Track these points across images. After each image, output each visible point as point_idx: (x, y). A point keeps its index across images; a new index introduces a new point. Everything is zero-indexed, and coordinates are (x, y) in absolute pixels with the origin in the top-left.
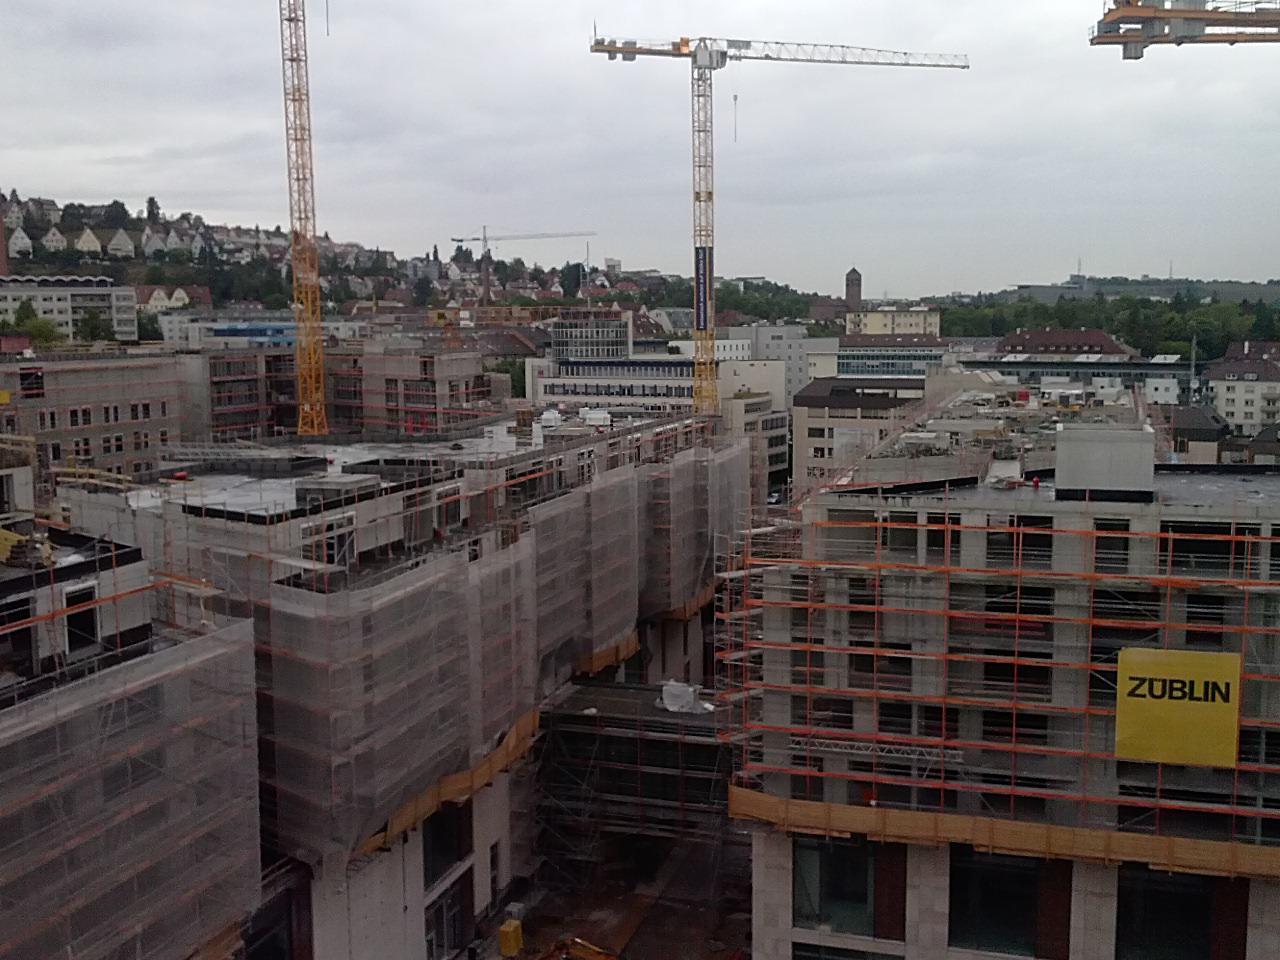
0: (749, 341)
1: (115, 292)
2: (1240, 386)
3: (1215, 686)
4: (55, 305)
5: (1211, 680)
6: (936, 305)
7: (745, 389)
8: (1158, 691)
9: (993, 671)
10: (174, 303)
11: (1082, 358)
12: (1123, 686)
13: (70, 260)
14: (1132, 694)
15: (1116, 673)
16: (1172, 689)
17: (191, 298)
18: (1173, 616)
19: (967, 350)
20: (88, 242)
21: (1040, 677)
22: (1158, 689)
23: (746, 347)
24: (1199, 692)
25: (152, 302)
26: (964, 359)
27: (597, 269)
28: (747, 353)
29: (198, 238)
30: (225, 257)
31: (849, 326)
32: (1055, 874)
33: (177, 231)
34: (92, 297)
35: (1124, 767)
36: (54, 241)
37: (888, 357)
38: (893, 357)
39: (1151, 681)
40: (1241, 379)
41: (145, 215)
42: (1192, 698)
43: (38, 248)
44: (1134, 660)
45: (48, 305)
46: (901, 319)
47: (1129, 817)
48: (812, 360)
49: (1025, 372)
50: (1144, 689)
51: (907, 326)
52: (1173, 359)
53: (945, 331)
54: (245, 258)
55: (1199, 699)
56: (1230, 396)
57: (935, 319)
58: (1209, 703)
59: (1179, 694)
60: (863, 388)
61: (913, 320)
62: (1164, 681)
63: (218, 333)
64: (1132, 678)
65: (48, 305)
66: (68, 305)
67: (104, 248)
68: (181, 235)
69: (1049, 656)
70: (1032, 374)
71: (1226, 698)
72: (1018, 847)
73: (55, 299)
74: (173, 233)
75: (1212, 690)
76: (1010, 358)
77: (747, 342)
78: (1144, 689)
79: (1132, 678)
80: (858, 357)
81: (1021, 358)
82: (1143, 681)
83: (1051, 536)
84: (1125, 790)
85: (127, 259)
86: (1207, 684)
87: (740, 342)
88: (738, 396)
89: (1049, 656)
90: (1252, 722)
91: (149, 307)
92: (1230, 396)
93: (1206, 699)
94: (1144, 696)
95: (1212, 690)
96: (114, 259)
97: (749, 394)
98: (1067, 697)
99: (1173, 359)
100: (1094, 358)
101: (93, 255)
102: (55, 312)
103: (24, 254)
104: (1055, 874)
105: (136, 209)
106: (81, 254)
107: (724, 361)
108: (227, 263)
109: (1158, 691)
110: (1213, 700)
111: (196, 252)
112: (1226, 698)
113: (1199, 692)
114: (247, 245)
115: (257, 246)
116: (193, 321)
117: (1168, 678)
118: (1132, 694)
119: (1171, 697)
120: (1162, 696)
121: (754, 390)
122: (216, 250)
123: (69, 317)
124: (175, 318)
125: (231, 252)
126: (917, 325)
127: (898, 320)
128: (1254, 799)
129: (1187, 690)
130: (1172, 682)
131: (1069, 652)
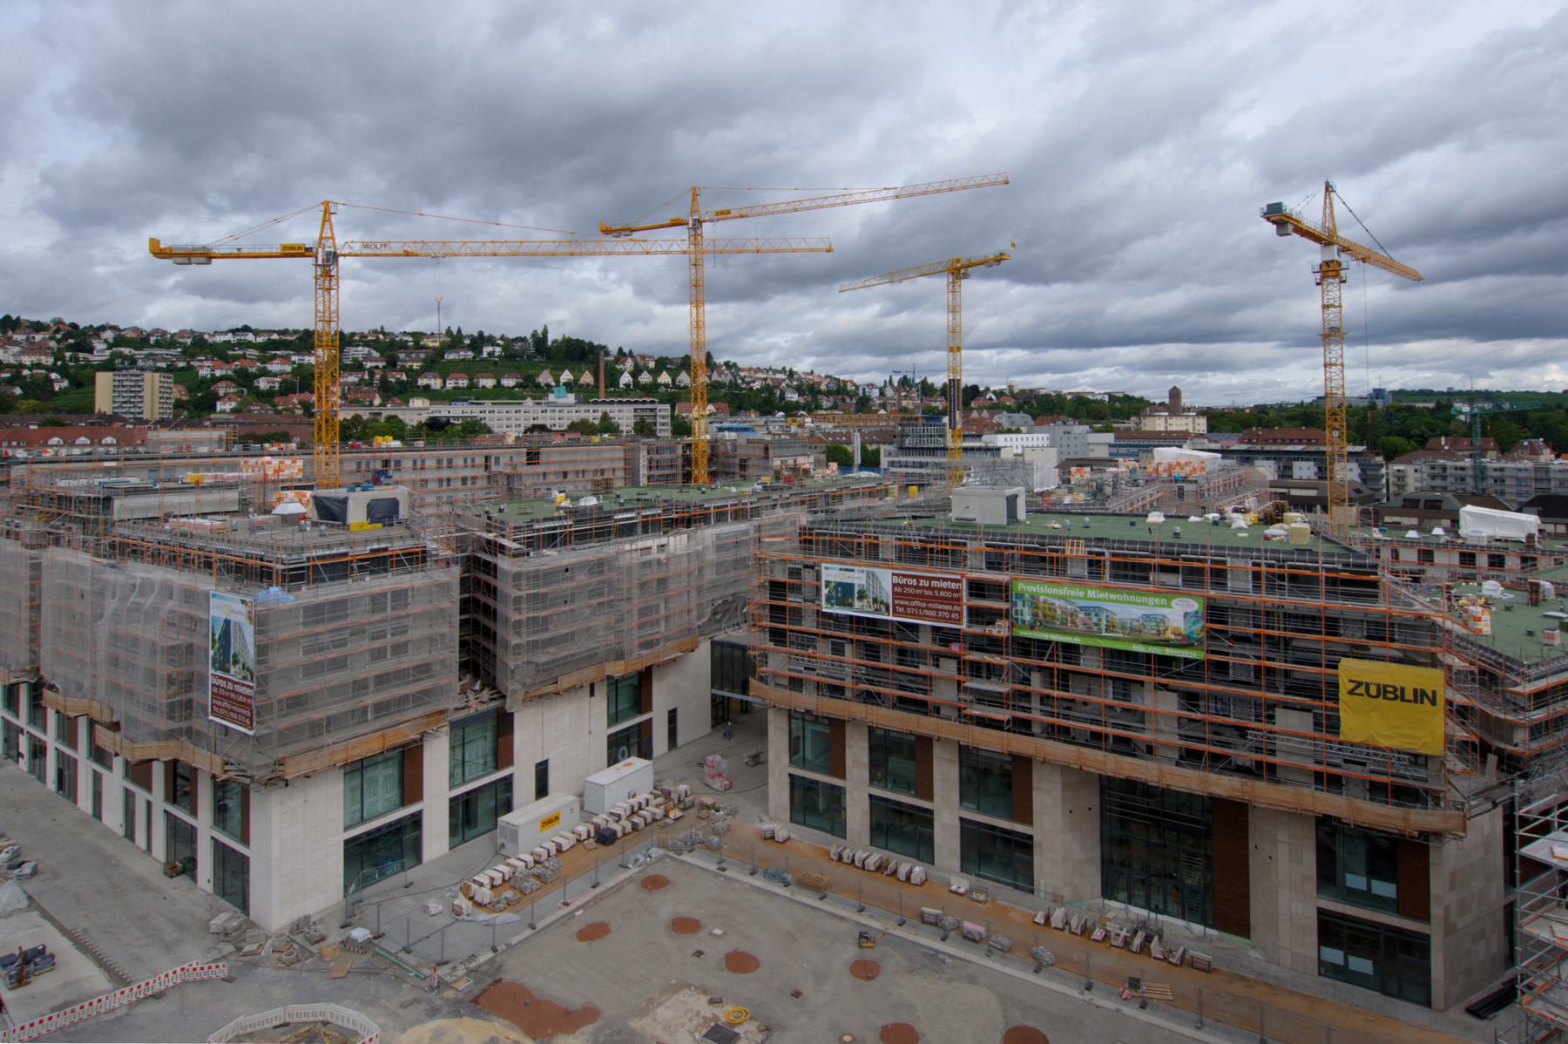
13: (651, 389)
20: (665, 378)
22: (1373, 691)
36: (645, 378)
43: (636, 383)
59: (1392, 696)
67: (674, 381)
85: (685, 387)
96: (678, 387)
101: (666, 386)
103: (627, 385)
117: (1382, 682)
120: (1377, 696)
127: (1169, 422)
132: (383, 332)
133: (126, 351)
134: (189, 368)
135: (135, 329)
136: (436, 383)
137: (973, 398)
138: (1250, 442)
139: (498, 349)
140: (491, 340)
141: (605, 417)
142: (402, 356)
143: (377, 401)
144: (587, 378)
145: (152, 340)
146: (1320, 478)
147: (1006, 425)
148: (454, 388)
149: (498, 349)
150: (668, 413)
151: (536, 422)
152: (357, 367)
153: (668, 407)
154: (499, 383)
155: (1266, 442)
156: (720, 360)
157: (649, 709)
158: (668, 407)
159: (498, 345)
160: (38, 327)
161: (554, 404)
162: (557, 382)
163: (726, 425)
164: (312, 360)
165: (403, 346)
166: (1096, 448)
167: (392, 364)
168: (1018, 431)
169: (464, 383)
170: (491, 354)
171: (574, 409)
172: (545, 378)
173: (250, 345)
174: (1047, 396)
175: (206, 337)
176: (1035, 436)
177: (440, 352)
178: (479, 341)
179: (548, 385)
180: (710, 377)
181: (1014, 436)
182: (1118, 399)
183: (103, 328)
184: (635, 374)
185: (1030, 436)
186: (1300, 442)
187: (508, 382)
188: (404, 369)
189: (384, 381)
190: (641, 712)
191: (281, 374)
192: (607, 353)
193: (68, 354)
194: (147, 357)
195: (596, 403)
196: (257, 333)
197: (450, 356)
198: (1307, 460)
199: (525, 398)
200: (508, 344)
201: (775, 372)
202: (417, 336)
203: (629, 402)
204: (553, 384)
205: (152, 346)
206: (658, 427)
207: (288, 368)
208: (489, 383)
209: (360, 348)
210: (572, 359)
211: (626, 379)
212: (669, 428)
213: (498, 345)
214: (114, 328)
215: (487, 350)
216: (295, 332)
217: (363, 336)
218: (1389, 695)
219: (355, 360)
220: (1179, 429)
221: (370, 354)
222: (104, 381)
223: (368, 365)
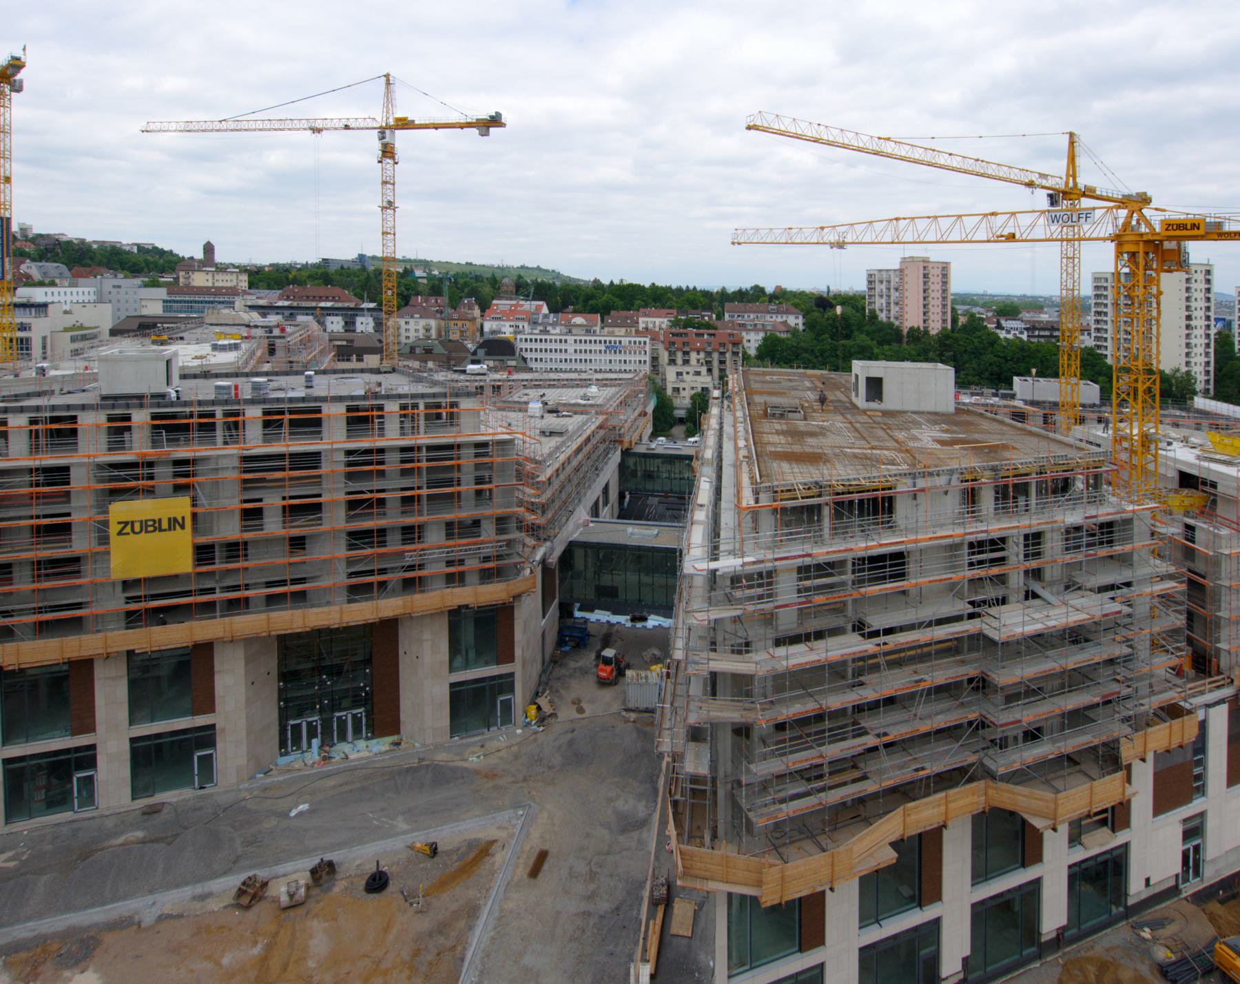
0: (95, 289)
2: (412, 321)
3: (175, 520)
5: (172, 516)
6: (243, 269)
7: (79, 324)
8: (137, 528)
9: (38, 531)
11: (323, 304)
12: (114, 529)
14: (120, 533)
15: (108, 521)
16: (147, 526)
18: (164, 476)
19: (252, 300)
21: (64, 530)
22: (137, 527)
23: (92, 293)
24: (165, 525)
26: (249, 304)
28: (93, 298)
31: (181, 280)
32: (83, 668)
35: (127, 584)
37: (188, 302)
38: (191, 302)
39: (133, 523)
40: (412, 317)
42: (161, 530)
44: (120, 510)
46: (220, 277)
47: (132, 619)
48: (144, 303)
49: (287, 313)
50: (128, 529)
51: (224, 281)
52: (372, 305)
53: (251, 285)
55: (165, 530)
56: (407, 327)
57: (245, 277)
58: (172, 532)
60: (162, 323)
61: (229, 277)
62: (141, 522)
64: (119, 523)
69: (69, 515)
70: (291, 314)
71: (183, 527)
72: (39, 659)
75: (174, 523)
76: (280, 304)
77: (92, 290)
78: (128, 529)
79: (119, 523)
80: (177, 302)
81: (286, 303)
82: (126, 523)
83: (6, 432)
84: (129, 600)
86: (169, 519)
87: (86, 290)
88: (66, 330)
89: (69, 515)
90: (202, 540)
92: (407, 327)
93: (170, 529)
94: (128, 534)
95: (174, 523)
97: (81, 327)
98: (80, 544)
99: (372, 305)
100: (329, 304)
104: (83, 668)
107: (53, 303)
109: (137, 528)
110: (175, 529)
112: (183, 527)
113: (165, 525)
117: (144, 518)
118: (120, 533)
119: (147, 532)
120: (141, 531)
121: (86, 325)
126: (231, 281)
128: (214, 589)
129: (157, 525)
130: (146, 521)
131: (81, 512)
138: (288, 299)
146: (346, 331)
155: (301, 299)
166: (149, 304)
168: (53, 284)
174: (69, 243)
176: (80, 290)
181: (49, 290)
182: (148, 251)
185: (69, 290)
186: (327, 299)
198: (337, 315)
218: (151, 529)
220: (229, 284)
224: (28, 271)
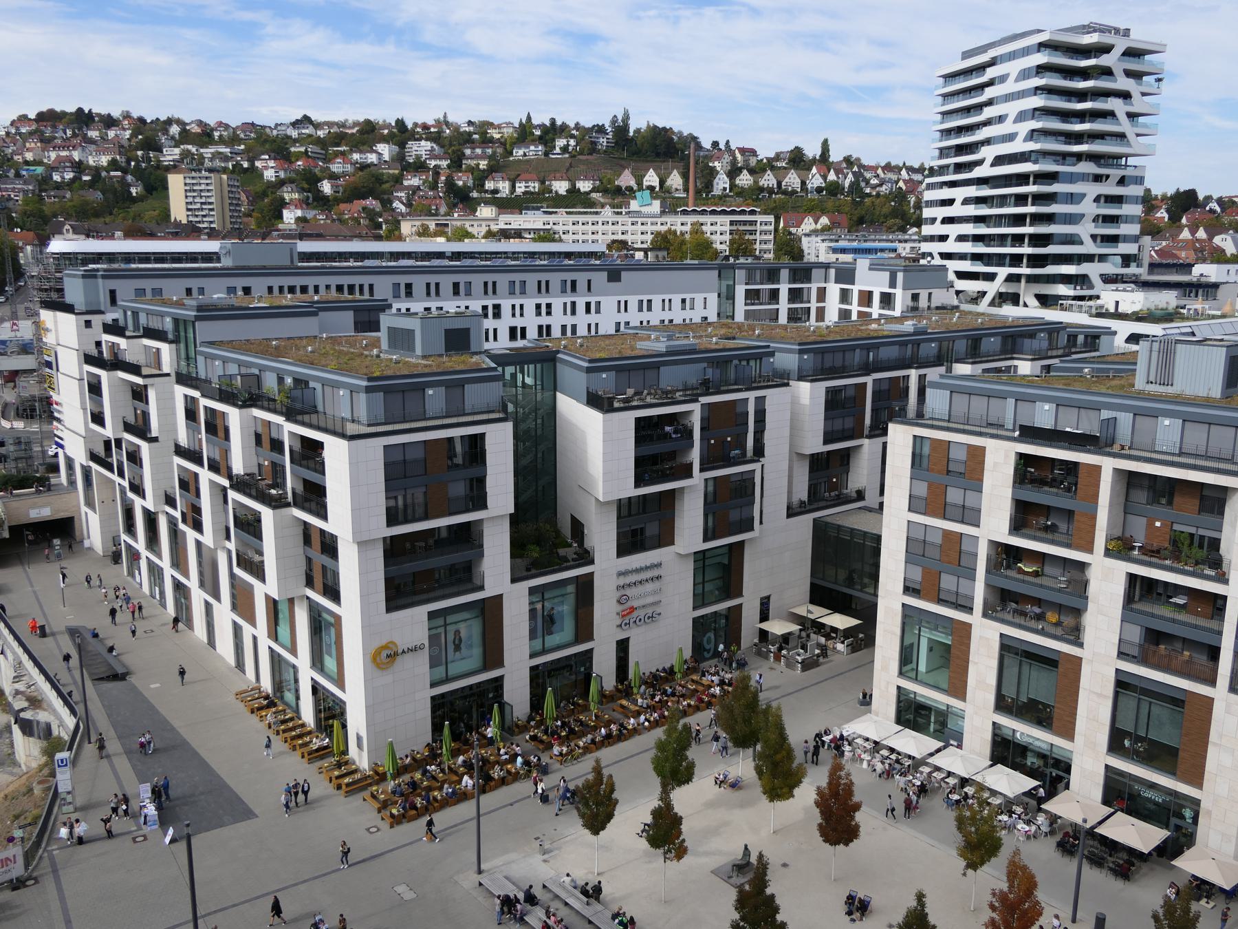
1: (759, 218)
4: (718, 228)
10: (819, 227)
17: (833, 223)
20: (769, 180)
25: (803, 226)
27: (1192, 194)
29: (850, 176)
30: (868, 190)
33: (835, 170)
34: (745, 223)
36: (745, 179)
41: (818, 158)
45: (714, 228)
54: (884, 189)
63: (835, 251)
65: (714, 228)
66: (727, 228)
67: (779, 184)
68: (837, 173)
73: (600, 223)
74: (832, 171)
91: (800, 230)
96: (785, 193)
101: (770, 191)
102: (600, 233)
105: (812, 150)
106: (762, 189)
108: (869, 195)
111: (847, 184)
114: (890, 181)
115: (897, 182)
116: (823, 240)
122: (863, 184)
123: (727, 237)
124: (813, 238)
125: (874, 187)
132: (447, 123)
133: (193, 149)
134: (253, 168)
135: (200, 123)
136: (504, 187)
137: (1185, 210)
139: (572, 142)
140: (563, 130)
141: (697, 229)
142: (468, 152)
143: (443, 210)
144: (675, 180)
145: (216, 134)
147: (1230, 249)
148: (525, 193)
149: (572, 142)
150: (772, 228)
151: (615, 237)
152: (419, 166)
153: (771, 218)
154: (574, 185)
156: (835, 156)
157: (739, 594)
158: (771, 218)
159: (572, 136)
160: (109, 122)
161: (638, 214)
162: (640, 183)
163: (843, 244)
164: (372, 158)
165: (466, 139)
167: (457, 163)
169: (535, 186)
170: (565, 149)
171: (659, 220)
172: (626, 179)
173: (310, 139)
175: (268, 130)
177: (507, 146)
178: (553, 131)
179: (630, 189)
180: (825, 177)
183: (169, 122)
184: (733, 172)
187: (584, 186)
188: (471, 170)
189: (450, 184)
190: (729, 596)
191: (344, 174)
192: (699, 146)
193: (140, 153)
194: (216, 155)
195: (685, 212)
196: (317, 126)
197: (519, 153)
199: (603, 206)
200: (588, 136)
201: (911, 170)
202: (484, 126)
203: (724, 212)
204: (635, 187)
205: (216, 143)
206: (757, 246)
207: (349, 168)
208: (561, 187)
209: (423, 143)
210: (658, 155)
211: (721, 183)
212: (771, 246)
213: (572, 136)
214: (179, 122)
215: (561, 143)
216: (356, 124)
217: (425, 127)
219: (418, 157)
221: (432, 150)
222: (176, 183)
223: (433, 163)
224: (1222, 244)
